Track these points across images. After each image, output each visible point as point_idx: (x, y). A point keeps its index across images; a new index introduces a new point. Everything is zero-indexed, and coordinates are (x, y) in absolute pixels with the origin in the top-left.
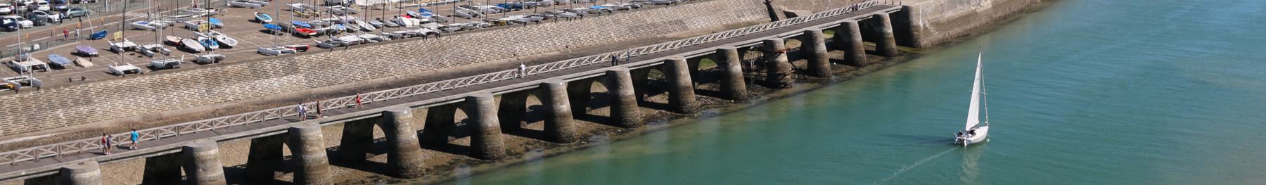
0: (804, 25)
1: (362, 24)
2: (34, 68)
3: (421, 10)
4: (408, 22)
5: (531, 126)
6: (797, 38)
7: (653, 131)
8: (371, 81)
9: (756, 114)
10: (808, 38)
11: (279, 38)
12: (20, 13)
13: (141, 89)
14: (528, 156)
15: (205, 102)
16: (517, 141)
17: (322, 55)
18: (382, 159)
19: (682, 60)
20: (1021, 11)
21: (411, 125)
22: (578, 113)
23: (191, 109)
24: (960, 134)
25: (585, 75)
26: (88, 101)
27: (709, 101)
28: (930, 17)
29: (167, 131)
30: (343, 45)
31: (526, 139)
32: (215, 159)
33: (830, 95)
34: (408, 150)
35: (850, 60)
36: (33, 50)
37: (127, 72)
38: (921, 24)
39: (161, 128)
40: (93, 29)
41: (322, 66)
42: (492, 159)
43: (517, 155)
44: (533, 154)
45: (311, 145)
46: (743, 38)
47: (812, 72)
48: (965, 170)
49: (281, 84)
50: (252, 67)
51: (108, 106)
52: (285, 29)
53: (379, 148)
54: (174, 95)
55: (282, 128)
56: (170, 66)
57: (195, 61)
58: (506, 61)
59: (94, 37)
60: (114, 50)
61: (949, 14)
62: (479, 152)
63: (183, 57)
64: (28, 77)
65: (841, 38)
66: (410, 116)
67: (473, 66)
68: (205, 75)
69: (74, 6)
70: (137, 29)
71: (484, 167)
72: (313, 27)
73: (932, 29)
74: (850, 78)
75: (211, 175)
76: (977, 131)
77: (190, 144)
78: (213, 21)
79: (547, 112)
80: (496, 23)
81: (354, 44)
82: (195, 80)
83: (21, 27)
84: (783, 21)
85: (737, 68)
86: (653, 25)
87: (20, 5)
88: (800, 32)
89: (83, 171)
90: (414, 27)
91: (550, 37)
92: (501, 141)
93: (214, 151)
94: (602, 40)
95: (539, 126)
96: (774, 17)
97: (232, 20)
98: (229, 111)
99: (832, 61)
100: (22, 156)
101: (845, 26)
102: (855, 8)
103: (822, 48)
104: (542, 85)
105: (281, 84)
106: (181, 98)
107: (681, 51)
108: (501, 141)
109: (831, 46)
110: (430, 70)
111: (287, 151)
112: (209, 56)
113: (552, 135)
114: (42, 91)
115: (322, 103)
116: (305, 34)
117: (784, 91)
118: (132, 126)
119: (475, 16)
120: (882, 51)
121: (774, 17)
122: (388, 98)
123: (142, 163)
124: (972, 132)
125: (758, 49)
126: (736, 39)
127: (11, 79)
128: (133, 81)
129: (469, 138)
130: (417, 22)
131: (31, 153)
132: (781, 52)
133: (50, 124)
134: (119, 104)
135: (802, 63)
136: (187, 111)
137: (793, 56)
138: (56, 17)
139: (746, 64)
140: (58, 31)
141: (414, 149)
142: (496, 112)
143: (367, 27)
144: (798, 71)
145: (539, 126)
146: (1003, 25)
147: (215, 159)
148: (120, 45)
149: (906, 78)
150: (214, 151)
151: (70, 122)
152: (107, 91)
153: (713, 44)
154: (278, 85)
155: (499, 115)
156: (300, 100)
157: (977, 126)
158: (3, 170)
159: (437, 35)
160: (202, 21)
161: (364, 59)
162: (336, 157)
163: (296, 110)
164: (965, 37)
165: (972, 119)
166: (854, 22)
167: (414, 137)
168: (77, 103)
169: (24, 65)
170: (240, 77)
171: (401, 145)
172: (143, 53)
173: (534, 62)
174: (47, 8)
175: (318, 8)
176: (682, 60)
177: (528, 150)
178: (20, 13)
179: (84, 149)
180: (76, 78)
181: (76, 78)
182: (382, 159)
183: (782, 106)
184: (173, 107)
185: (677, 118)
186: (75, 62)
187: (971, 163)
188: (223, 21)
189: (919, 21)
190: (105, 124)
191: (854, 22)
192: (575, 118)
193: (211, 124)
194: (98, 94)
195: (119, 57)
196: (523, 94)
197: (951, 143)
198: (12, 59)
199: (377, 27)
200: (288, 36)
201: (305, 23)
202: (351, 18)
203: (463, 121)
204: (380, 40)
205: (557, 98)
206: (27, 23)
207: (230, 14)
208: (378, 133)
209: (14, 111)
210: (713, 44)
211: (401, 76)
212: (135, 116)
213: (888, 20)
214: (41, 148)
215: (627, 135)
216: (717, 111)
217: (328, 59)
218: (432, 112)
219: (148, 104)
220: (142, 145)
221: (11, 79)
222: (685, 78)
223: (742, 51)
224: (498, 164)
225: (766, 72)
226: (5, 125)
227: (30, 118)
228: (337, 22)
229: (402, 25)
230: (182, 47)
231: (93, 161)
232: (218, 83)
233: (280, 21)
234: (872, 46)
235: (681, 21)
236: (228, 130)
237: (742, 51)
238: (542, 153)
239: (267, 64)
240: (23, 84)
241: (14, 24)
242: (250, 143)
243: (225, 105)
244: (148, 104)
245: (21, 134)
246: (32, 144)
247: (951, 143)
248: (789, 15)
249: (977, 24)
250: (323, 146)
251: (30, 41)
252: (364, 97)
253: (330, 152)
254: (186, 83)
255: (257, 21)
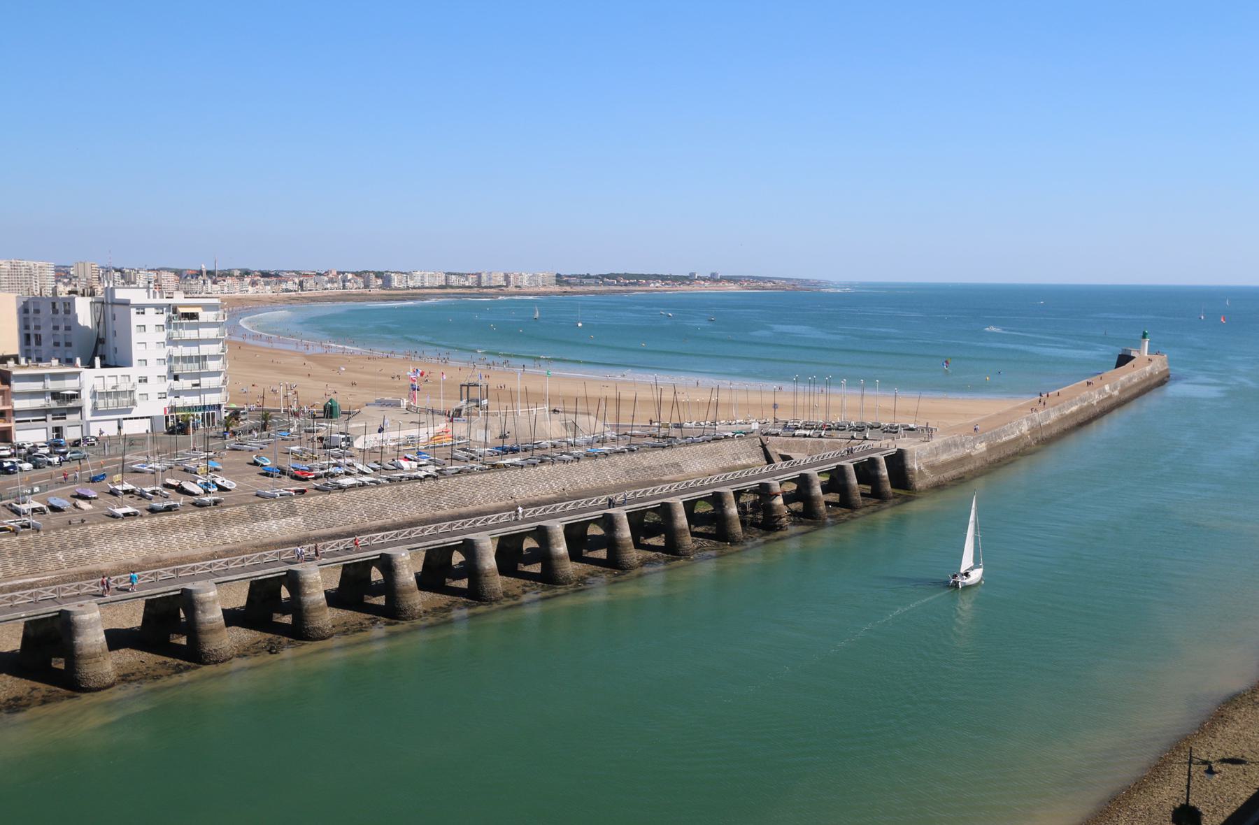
0: (799, 468)
1: (360, 467)
2: (34, 510)
3: (419, 453)
4: (405, 464)
5: (528, 569)
6: (793, 480)
7: (650, 573)
8: (369, 524)
9: (752, 556)
10: (804, 481)
11: (277, 480)
12: (20, 456)
13: (140, 532)
14: (525, 598)
15: (203, 545)
16: (514, 583)
17: (320, 498)
18: (380, 600)
19: (678, 502)
20: (1016, 454)
21: (408, 567)
22: (575, 555)
23: (190, 551)
24: (955, 576)
25: (581, 517)
26: (88, 544)
27: (705, 543)
28: (925, 460)
29: (166, 573)
30: (341, 488)
31: (522, 582)
32: (214, 601)
33: (825, 537)
34: (405, 592)
35: (846, 502)
36: (32, 493)
37: (127, 515)
38: (916, 467)
39: (160, 570)
40: (92, 472)
41: (320, 508)
42: (490, 601)
43: (515, 597)
44: (530, 596)
45: (310, 587)
46: (739, 481)
47: (808, 514)
48: (960, 612)
49: (280, 527)
50: (251, 510)
51: (107, 548)
52: (283, 472)
53: (377, 590)
54: (173, 538)
55: (281, 570)
56: (169, 509)
57: (194, 504)
58: (503, 503)
59: (93, 480)
60: (113, 493)
61: (944, 457)
62: (476, 594)
63: (182, 499)
64: (28, 520)
65: (836, 481)
66: (408, 558)
67: (471, 508)
68: (204, 518)
69: (74, 449)
70: (136, 472)
71: (481, 609)
72: (311, 469)
73: (927, 472)
74: (845, 521)
75: (210, 617)
76: (971, 573)
77: (189, 586)
78: (212, 464)
79: (544, 554)
80: (494, 466)
81: (352, 487)
82: (194, 523)
83: (21, 469)
84: (779, 464)
85: (733, 511)
86: (650, 468)
87: (20, 448)
88: (795, 474)
89: (83, 613)
90: (412, 470)
91: (547, 480)
92: (498, 583)
93: (213, 593)
94: (598, 483)
95: (536, 568)
96: (769, 460)
97: (230, 464)
98: (228, 553)
99: (827, 503)
100: (22, 597)
101: (841, 469)
102: (850, 451)
103: (818, 490)
104: (539, 527)
105: (280, 527)
106: (180, 541)
107: (677, 493)
108: (498, 583)
109: (826, 489)
110: (427, 513)
111: (285, 593)
112: (208, 499)
113: (549, 577)
114: (42, 534)
115: (320, 545)
116: (304, 476)
117: (780, 534)
118: (131, 569)
119: (472, 459)
120: (877, 494)
121: (769, 460)
122: (386, 540)
123: (140, 606)
124: (967, 574)
125: (754, 491)
126: (731, 482)
127: (11, 522)
128: (132, 523)
129: (466, 580)
130: (414, 465)
131: (31, 595)
132: (777, 495)
133: (50, 566)
134: (118, 546)
135: (797, 506)
136: (186, 553)
137: (788, 499)
138: (56, 459)
139: (741, 507)
140: (58, 474)
141: (412, 591)
142: (493, 554)
143: (365, 469)
144: (793, 513)
145: (536, 568)
146: (998, 467)
147: (214, 601)
148: (119, 487)
149: (901, 521)
150: (213, 593)
151: (70, 564)
152: (107, 534)
153: (709, 486)
154: (277, 527)
155: (496, 557)
156: (298, 543)
157: (972, 569)
158: (3, 612)
159: (435, 478)
160: (202, 464)
161: (362, 502)
162: (334, 599)
163: (294, 552)
164: (960, 480)
165: (967, 561)
166: (849, 465)
167: (412, 579)
168: (76, 546)
169: (24, 507)
170: (239, 520)
171: (399, 587)
172: (142, 495)
173: (531, 505)
174: (46, 450)
175: (317, 451)
176: (678, 502)
177: (525, 592)
178: (20, 456)
179: (84, 591)
180: (76, 521)
181: (76, 521)
182: (380, 600)
183: (777, 548)
184: (172, 550)
185: (673, 560)
186: (75, 505)
187: (965, 605)
188: (222, 464)
189: (914, 464)
190: (104, 566)
191: (849, 465)
192: (572, 560)
193: (210, 566)
194: (98, 537)
195: (118, 499)
196: (521, 536)
197: (946, 585)
198: (12, 501)
199: (374, 470)
200: (286, 479)
201: (303, 466)
202: (349, 460)
203: (461, 563)
204: (378, 483)
205: (554, 541)
206: (27, 466)
207: (228, 457)
208: (376, 575)
209: (14, 554)
210: (709, 486)
211: (398, 519)
212: (135, 558)
213: (883, 463)
214: (41, 590)
215: (623, 577)
216: (713, 553)
217: (327, 502)
218: (430, 555)
219: (147, 547)
220: (141, 587)
221: (11, 522)
222: (682, 520)
223: (738, 494)
224: (495, 606)
225: (761, 515)
226: (5, 567)
227: (30, 560)
228: (335, 465)
229: (400, 468)
230: (181, 490)
231: (93, 603)
232: (217, 525)
233: (279, 464)
234: (867, 489)
235: (677, 464)
236: (227, 572)
237: (738, 494)
238: (539, 595)
239: (266, 507)
240: (23, 527)
241: (14, 467)
242: (248, 585)
243: (224, 547)
244: (147, 547)
245: (21, 576)
246: (32, 586)
247: (946, 585)
248: (785, 458)
249: (972, 467)
250: (322, 588)
251: (29, 483)
252: (362, 540)
253: (328, 594)
254: (185, 526)
255: (256, 464)
